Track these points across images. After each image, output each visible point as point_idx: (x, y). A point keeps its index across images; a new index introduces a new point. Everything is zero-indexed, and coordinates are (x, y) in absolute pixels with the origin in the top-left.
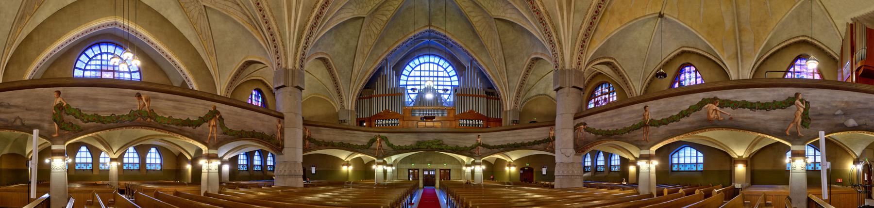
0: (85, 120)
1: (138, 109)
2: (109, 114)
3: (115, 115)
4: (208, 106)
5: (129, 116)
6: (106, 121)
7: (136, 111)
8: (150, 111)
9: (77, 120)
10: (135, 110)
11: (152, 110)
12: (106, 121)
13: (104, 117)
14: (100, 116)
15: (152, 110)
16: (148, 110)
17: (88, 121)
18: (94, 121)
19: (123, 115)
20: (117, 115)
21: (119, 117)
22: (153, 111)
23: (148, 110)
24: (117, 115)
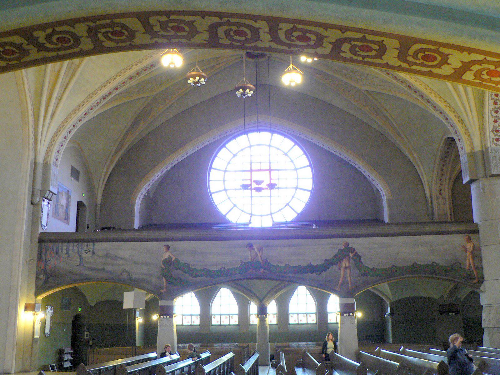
0: (194, 275)
1: (250, 260)
2: (218, 268)
3: (224, 268)
4: (337, 244)
5: (240, 268)
6: (215, 275)
7: (247, 263)
8: (263, 261)
9: (186, 274)
10: (246, 261)
11: (266, 260)
12: (215, 275)
13: (213, 272)
14: (209, 271)
15: (266, 260)
16: (260, 260)
17: (197, 276)
18: (204, 275)
19: (234, 268)
20: (226, 268)
21: (229, 270)
22: (267, 261)
23: (260, 260)
24: (226, 268)
